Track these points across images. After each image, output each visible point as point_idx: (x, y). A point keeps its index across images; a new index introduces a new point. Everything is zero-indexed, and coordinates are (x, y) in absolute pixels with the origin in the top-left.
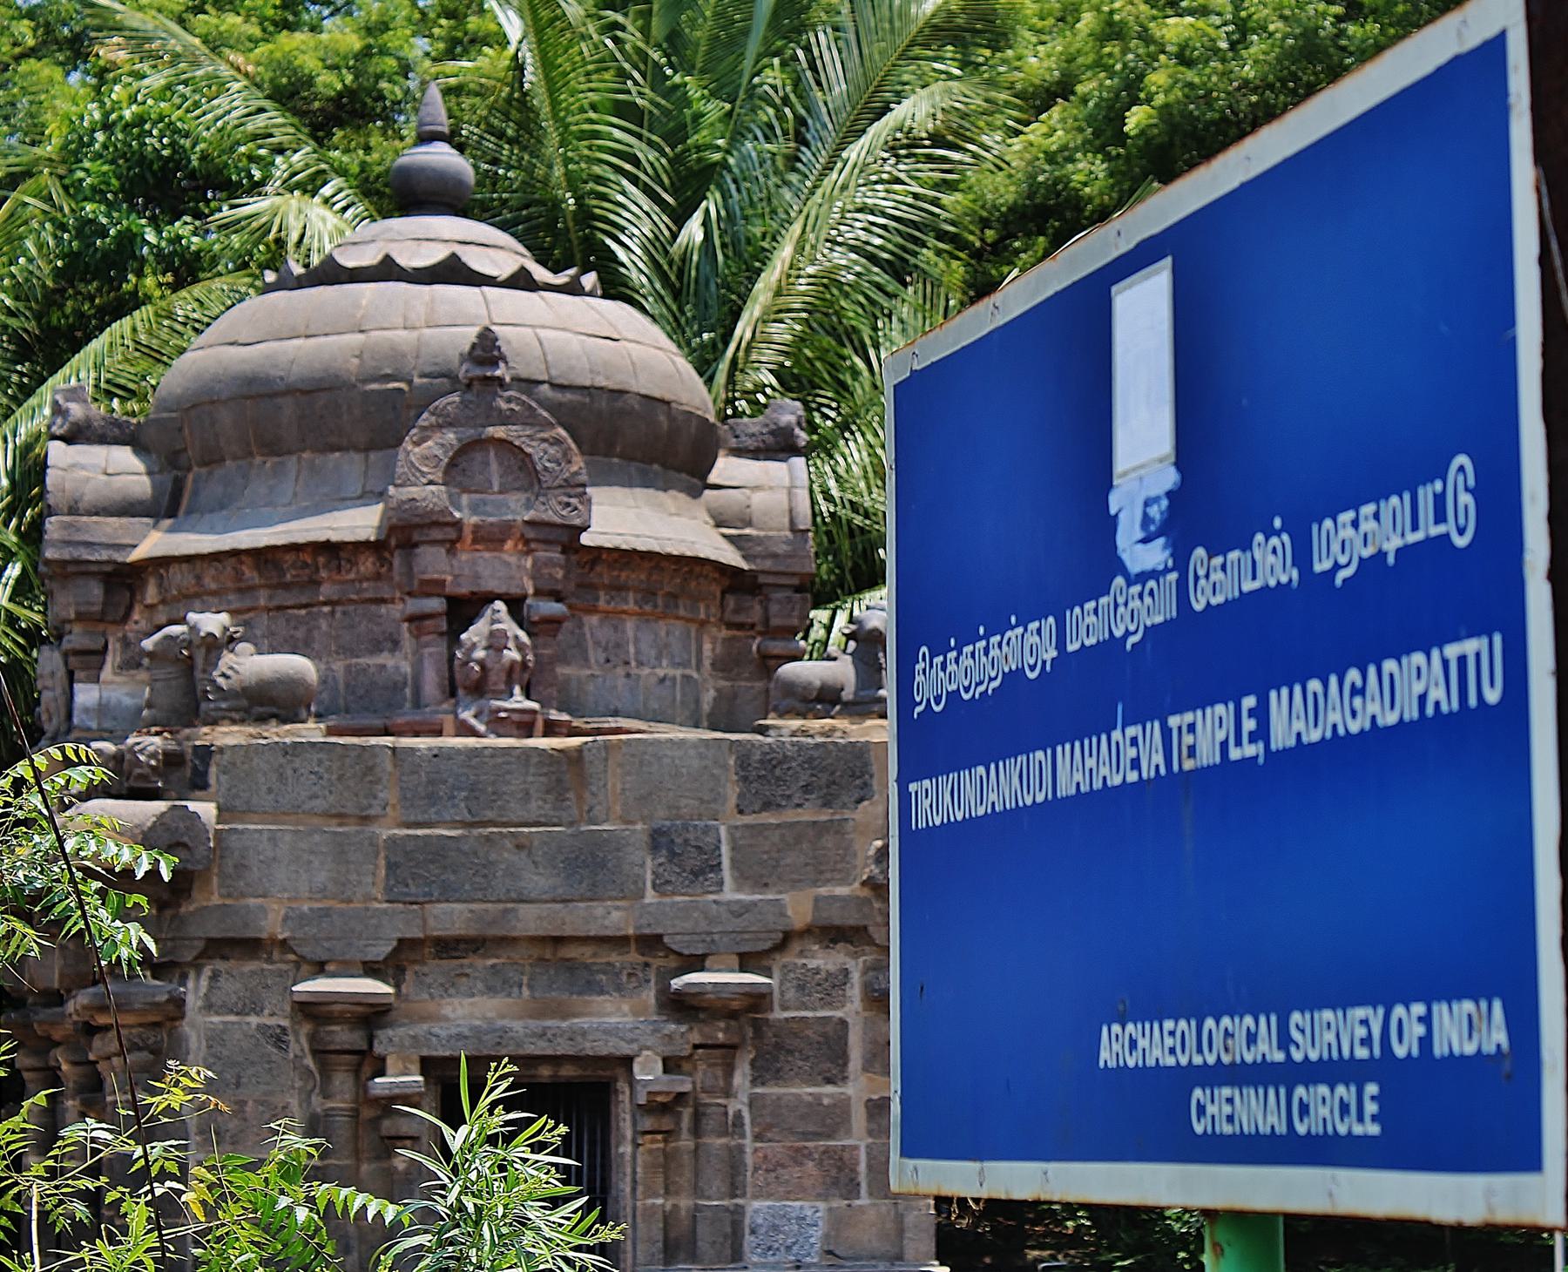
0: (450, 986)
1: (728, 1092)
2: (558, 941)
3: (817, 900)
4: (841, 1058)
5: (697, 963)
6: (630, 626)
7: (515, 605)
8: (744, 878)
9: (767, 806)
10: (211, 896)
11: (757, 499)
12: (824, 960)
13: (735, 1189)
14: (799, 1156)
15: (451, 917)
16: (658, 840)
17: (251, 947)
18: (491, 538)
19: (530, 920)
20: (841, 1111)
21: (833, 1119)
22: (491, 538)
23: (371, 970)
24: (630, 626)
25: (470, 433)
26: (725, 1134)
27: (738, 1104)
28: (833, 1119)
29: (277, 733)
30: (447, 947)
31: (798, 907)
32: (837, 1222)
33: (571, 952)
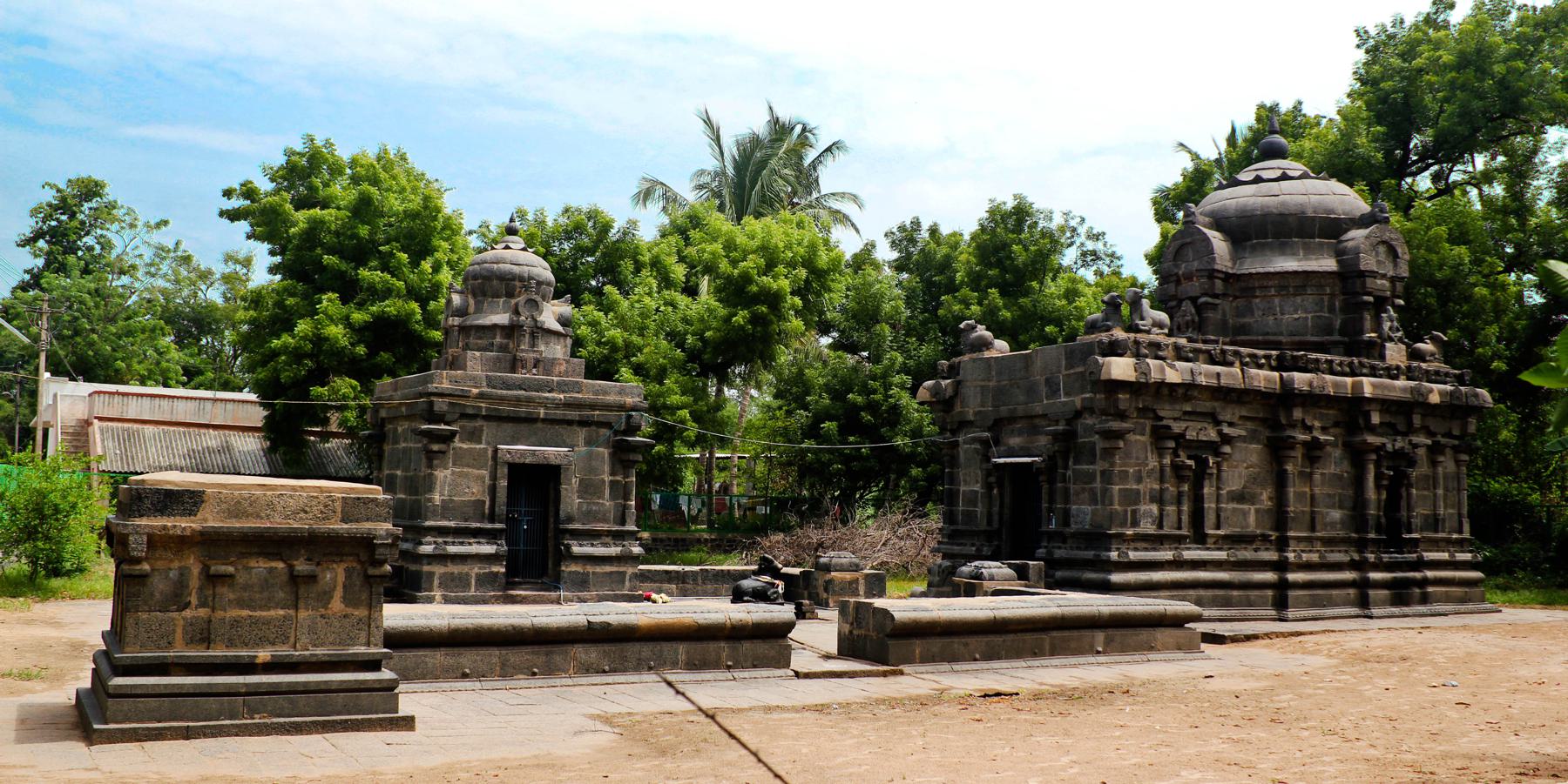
0: (1012, 433)
1: (1066, 467)
2: (1032, 417)
3: (1083, 400)
4: (1094, 456)
5: (1057, 422)
6: (1277, 301)
7: (1194, 300)
8: (1067, 394)
9: (1072, 367)
10: (958, 409)
11: (1350, 244)
12: (1089, 421)
13: (1067, 500)
14: (1084, 490)
15: (1004, 411)
16: (1047, 381)
17: (971, 423)
18: (1189, 277)
19: (1021, 410)
20: (1094, 473)
21: (1091, 477)
22: (1189, 277)
23: (989, 429)
24: (1277, 301)
25: (1179, 242)
26: (1064, 481)
27: (1070, 473)
28: (1091, 477)
29: (975, 355)
30: (1012, 419)
31: (1077, 401)
32: (1094, 513)
33: (1037, 421)
